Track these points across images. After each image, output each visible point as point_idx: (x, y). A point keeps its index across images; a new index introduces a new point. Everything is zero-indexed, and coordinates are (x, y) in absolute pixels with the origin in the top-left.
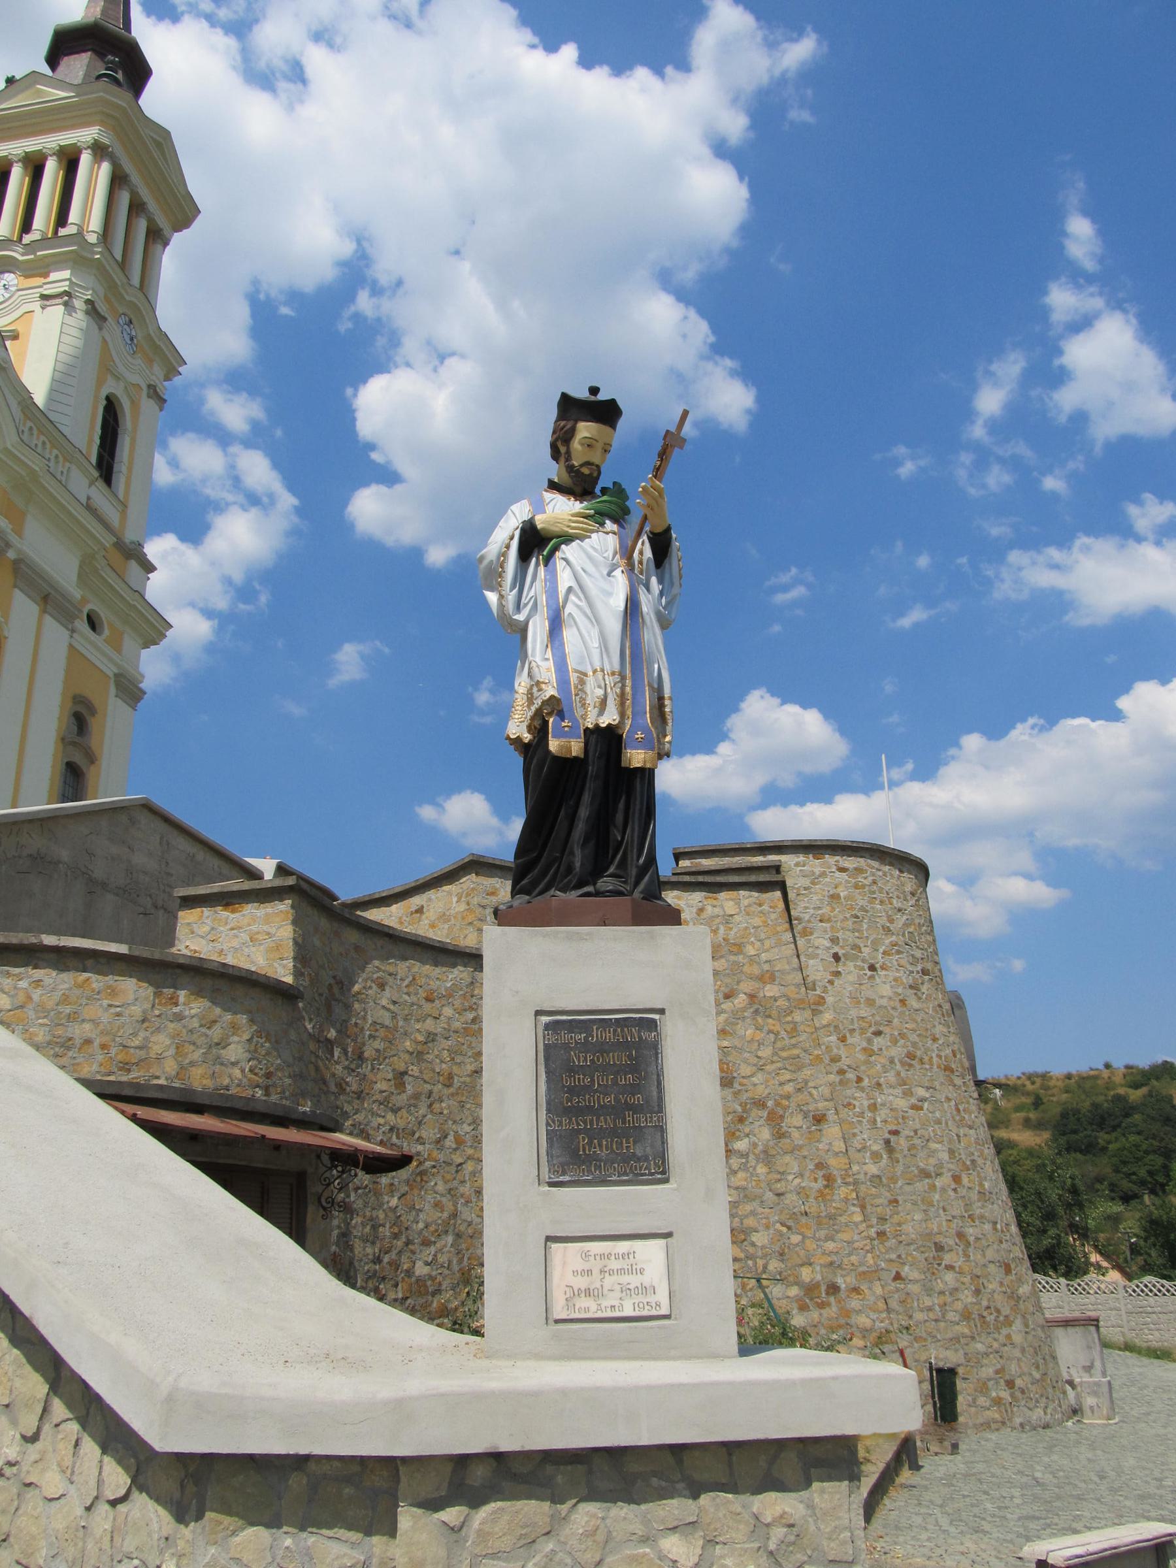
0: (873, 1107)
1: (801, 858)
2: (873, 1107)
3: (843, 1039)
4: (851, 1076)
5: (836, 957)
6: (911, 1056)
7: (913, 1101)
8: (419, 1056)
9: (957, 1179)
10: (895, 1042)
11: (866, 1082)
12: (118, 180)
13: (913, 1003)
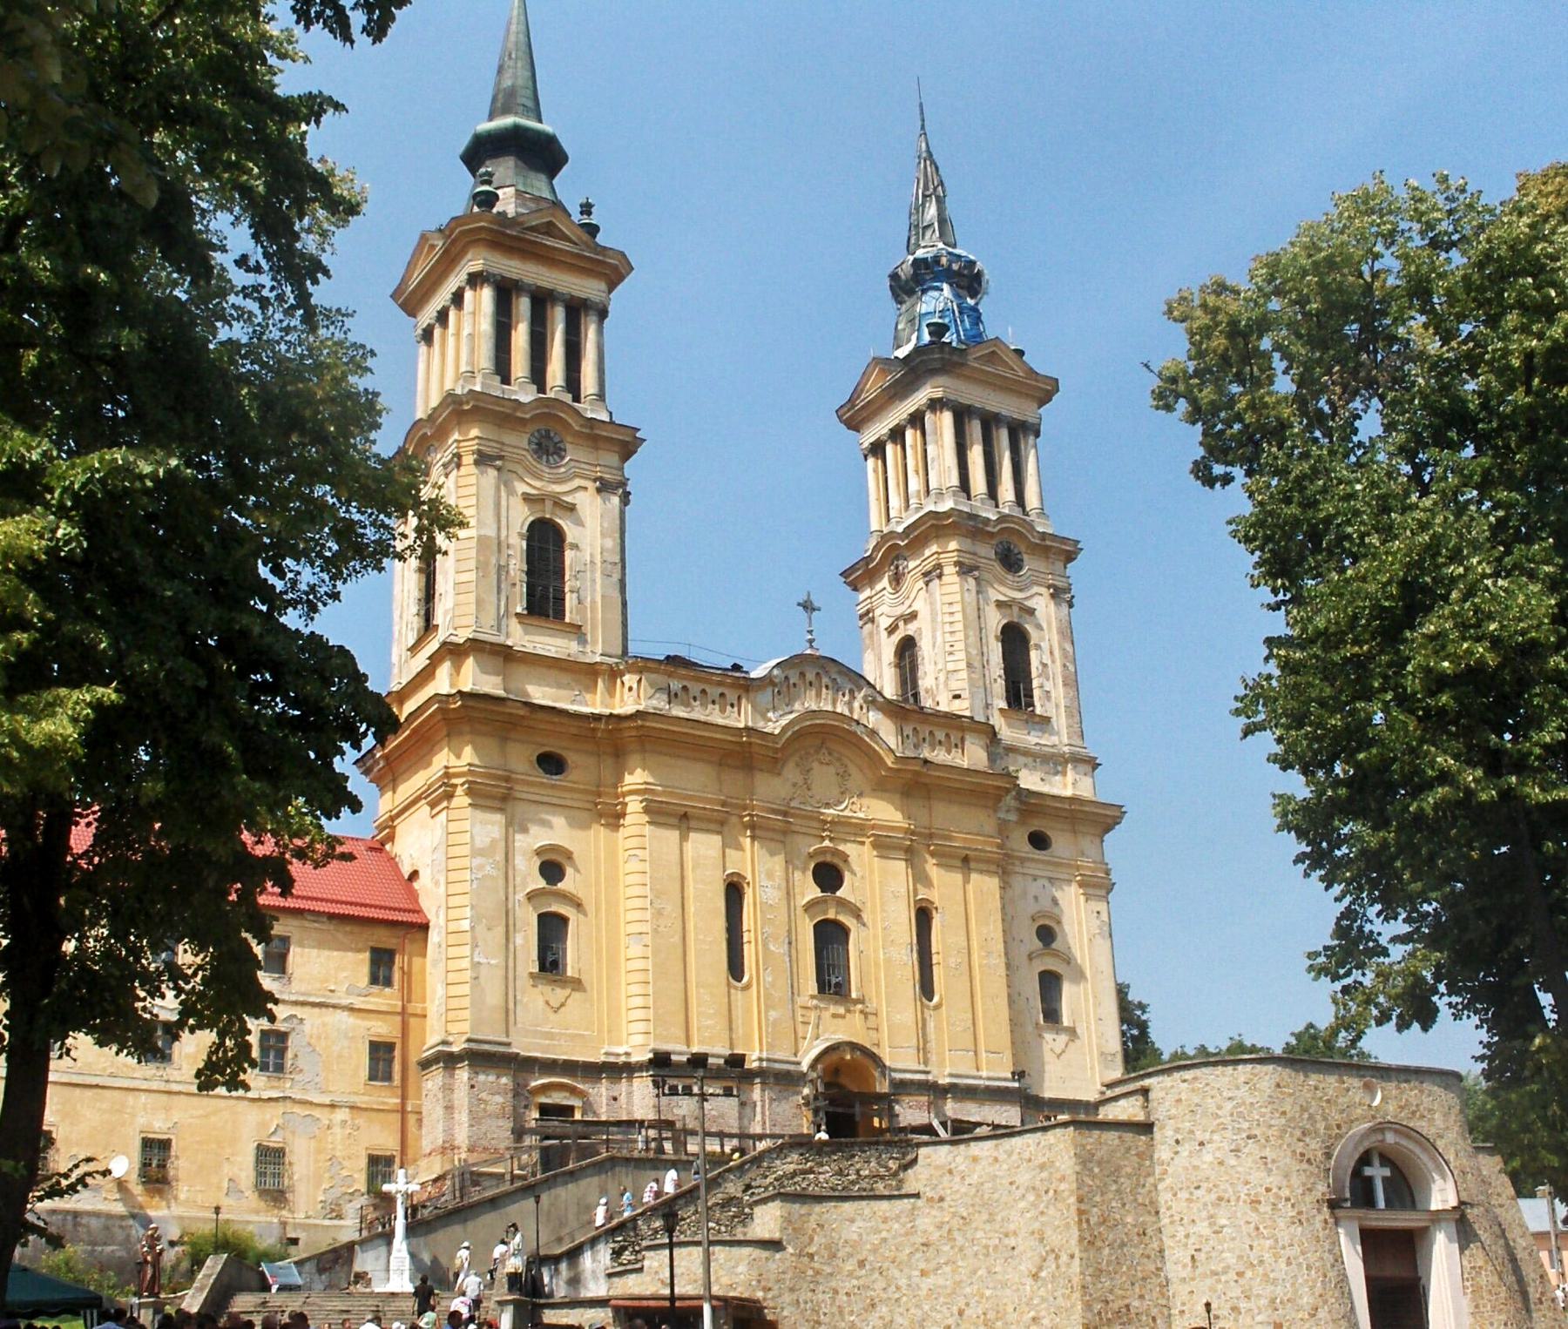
0: (1187, 1236)
1: (1160, 1078)
2: (1187, 1236)
3: (1175, 1195)
4: (1177, 1218)
5: (1177, 1142)
6: (1220, 1199)
7: (1216, 1228)
8: (875, 1251)
9: (1240, 1274)
10: (1210, 1191)
11: (1185, 1221)
12: (962, 415)
13: (1233, 1162)
